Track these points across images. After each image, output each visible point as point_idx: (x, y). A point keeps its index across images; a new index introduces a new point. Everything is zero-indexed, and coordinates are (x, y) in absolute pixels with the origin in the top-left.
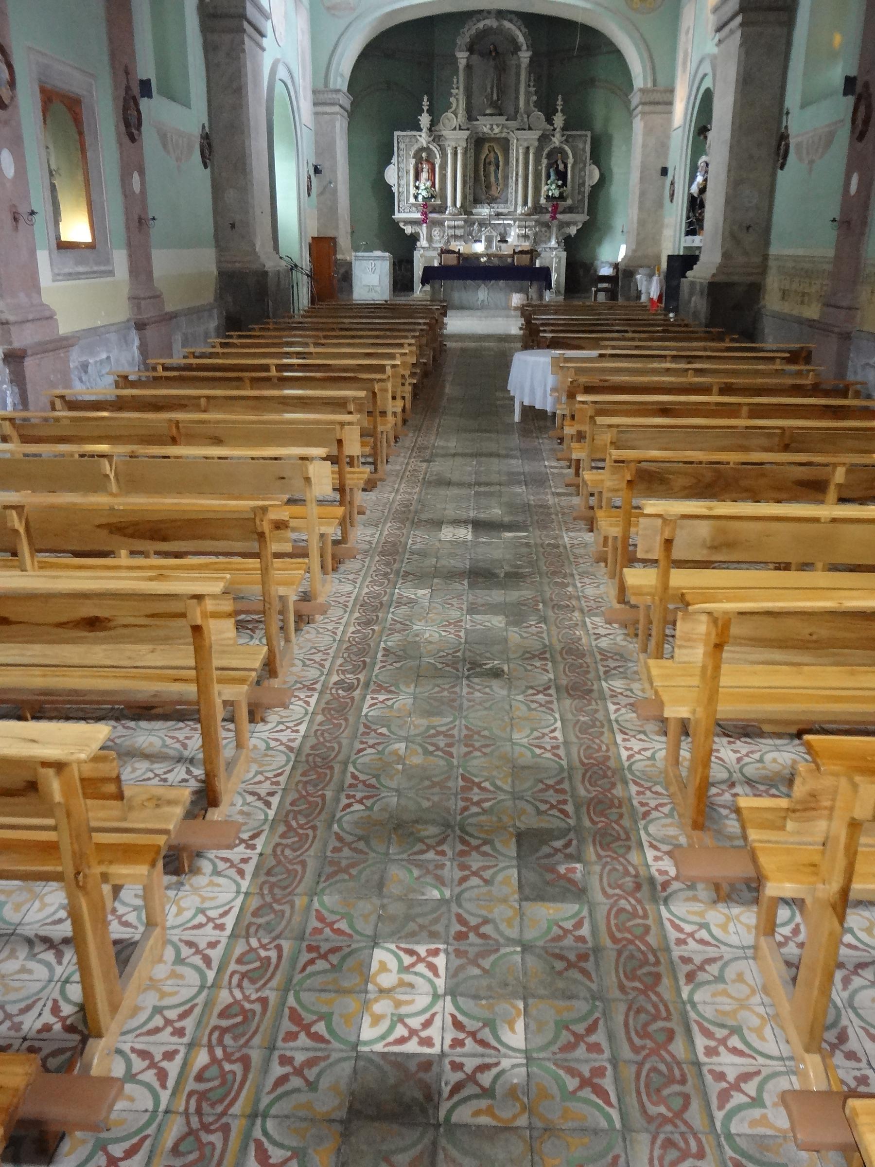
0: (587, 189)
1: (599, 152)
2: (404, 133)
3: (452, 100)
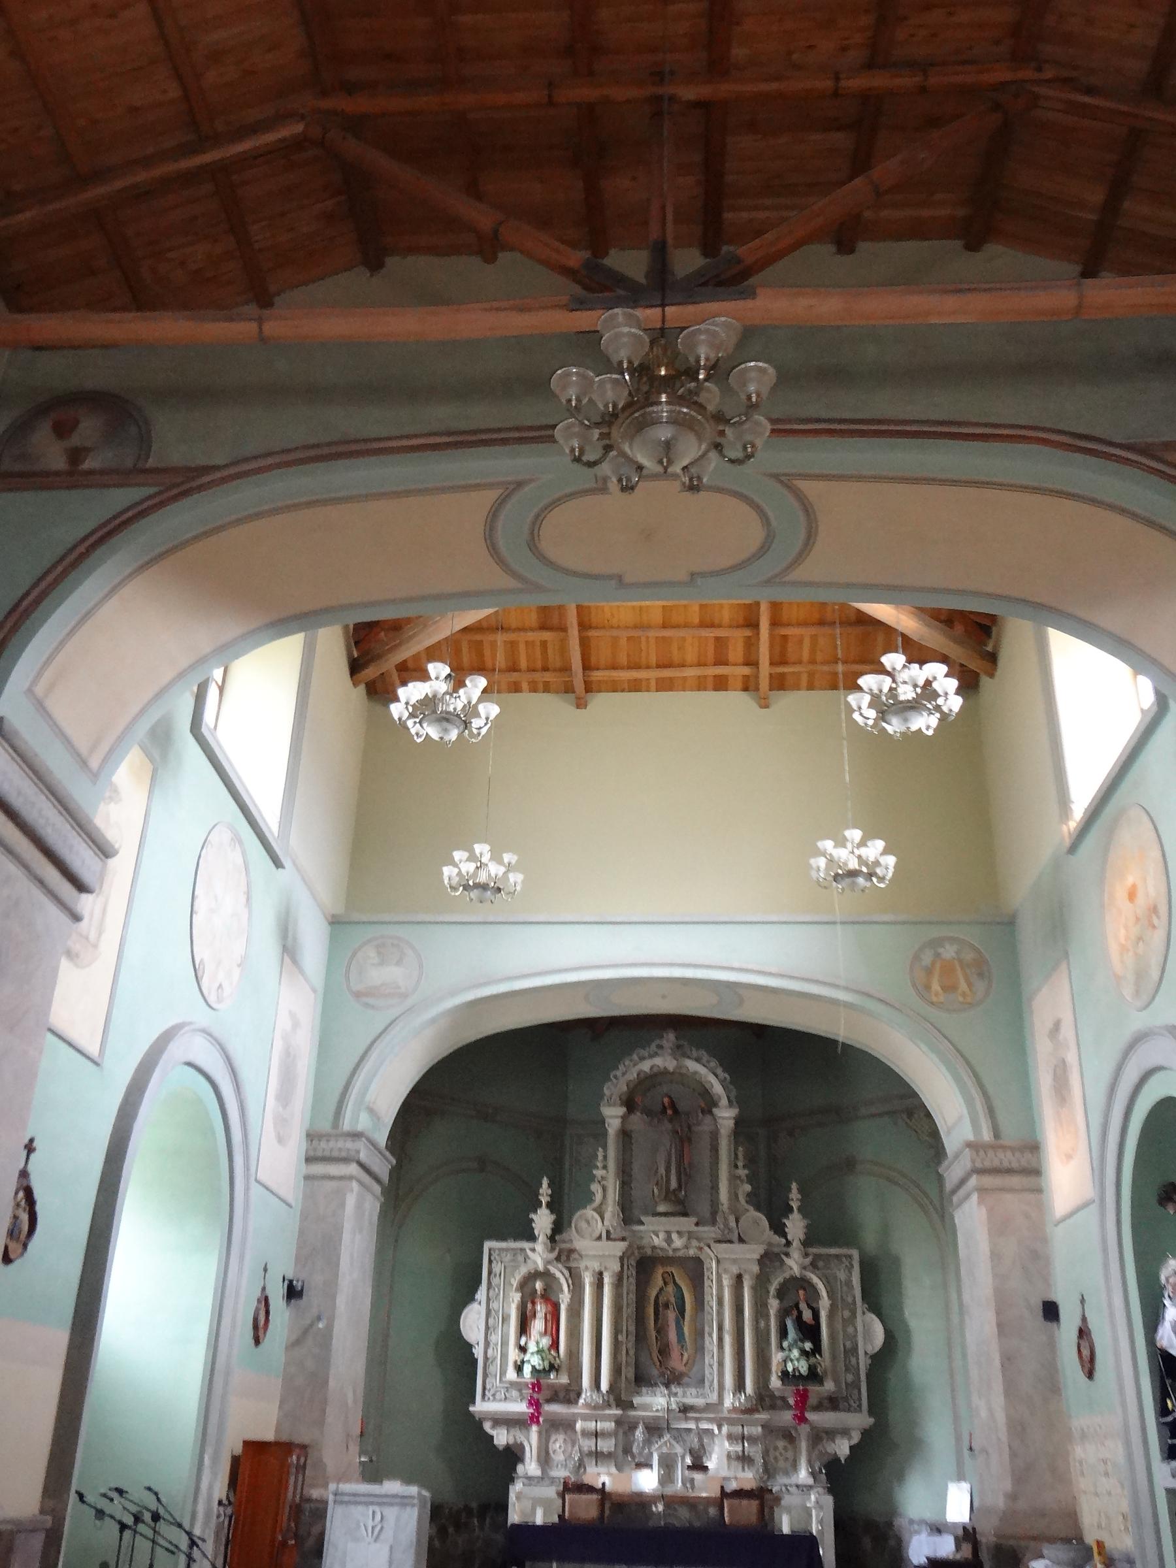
0: (863, 1363)
1: (878, 1287)
2: (503, 1245)
3: (595, 1187)
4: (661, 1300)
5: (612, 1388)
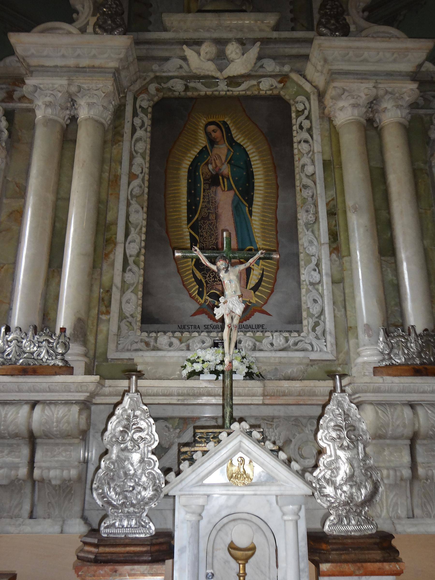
4: (204, 170)
5: (82, 330)
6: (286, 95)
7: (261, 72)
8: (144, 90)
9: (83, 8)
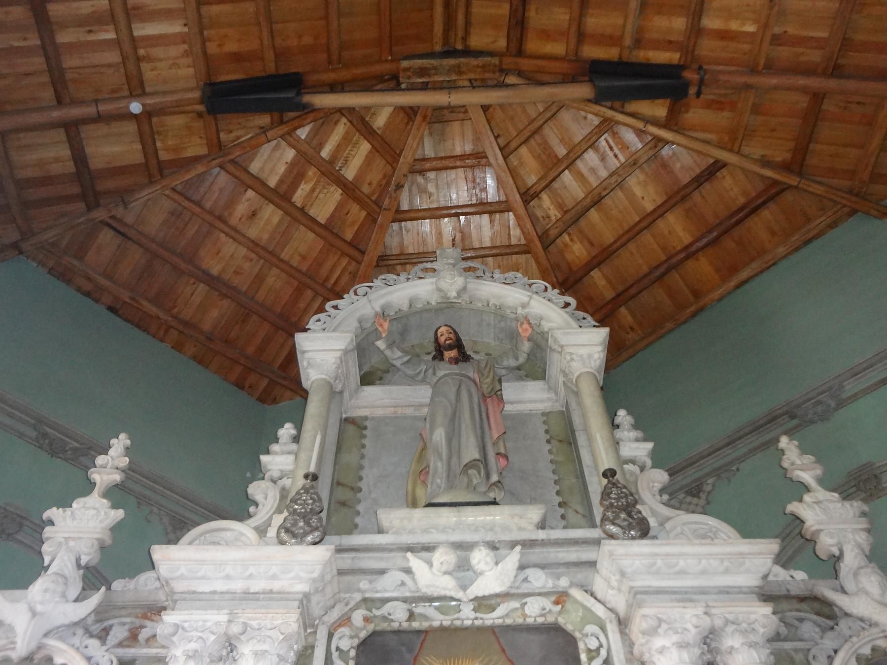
6: (568, 622)
7: (525, 588)
8: (345, 620)
9: (266, 498)
